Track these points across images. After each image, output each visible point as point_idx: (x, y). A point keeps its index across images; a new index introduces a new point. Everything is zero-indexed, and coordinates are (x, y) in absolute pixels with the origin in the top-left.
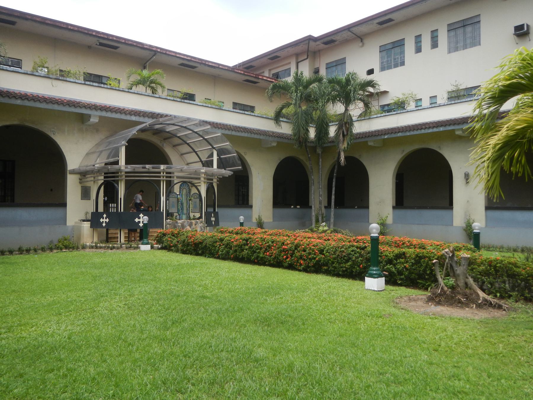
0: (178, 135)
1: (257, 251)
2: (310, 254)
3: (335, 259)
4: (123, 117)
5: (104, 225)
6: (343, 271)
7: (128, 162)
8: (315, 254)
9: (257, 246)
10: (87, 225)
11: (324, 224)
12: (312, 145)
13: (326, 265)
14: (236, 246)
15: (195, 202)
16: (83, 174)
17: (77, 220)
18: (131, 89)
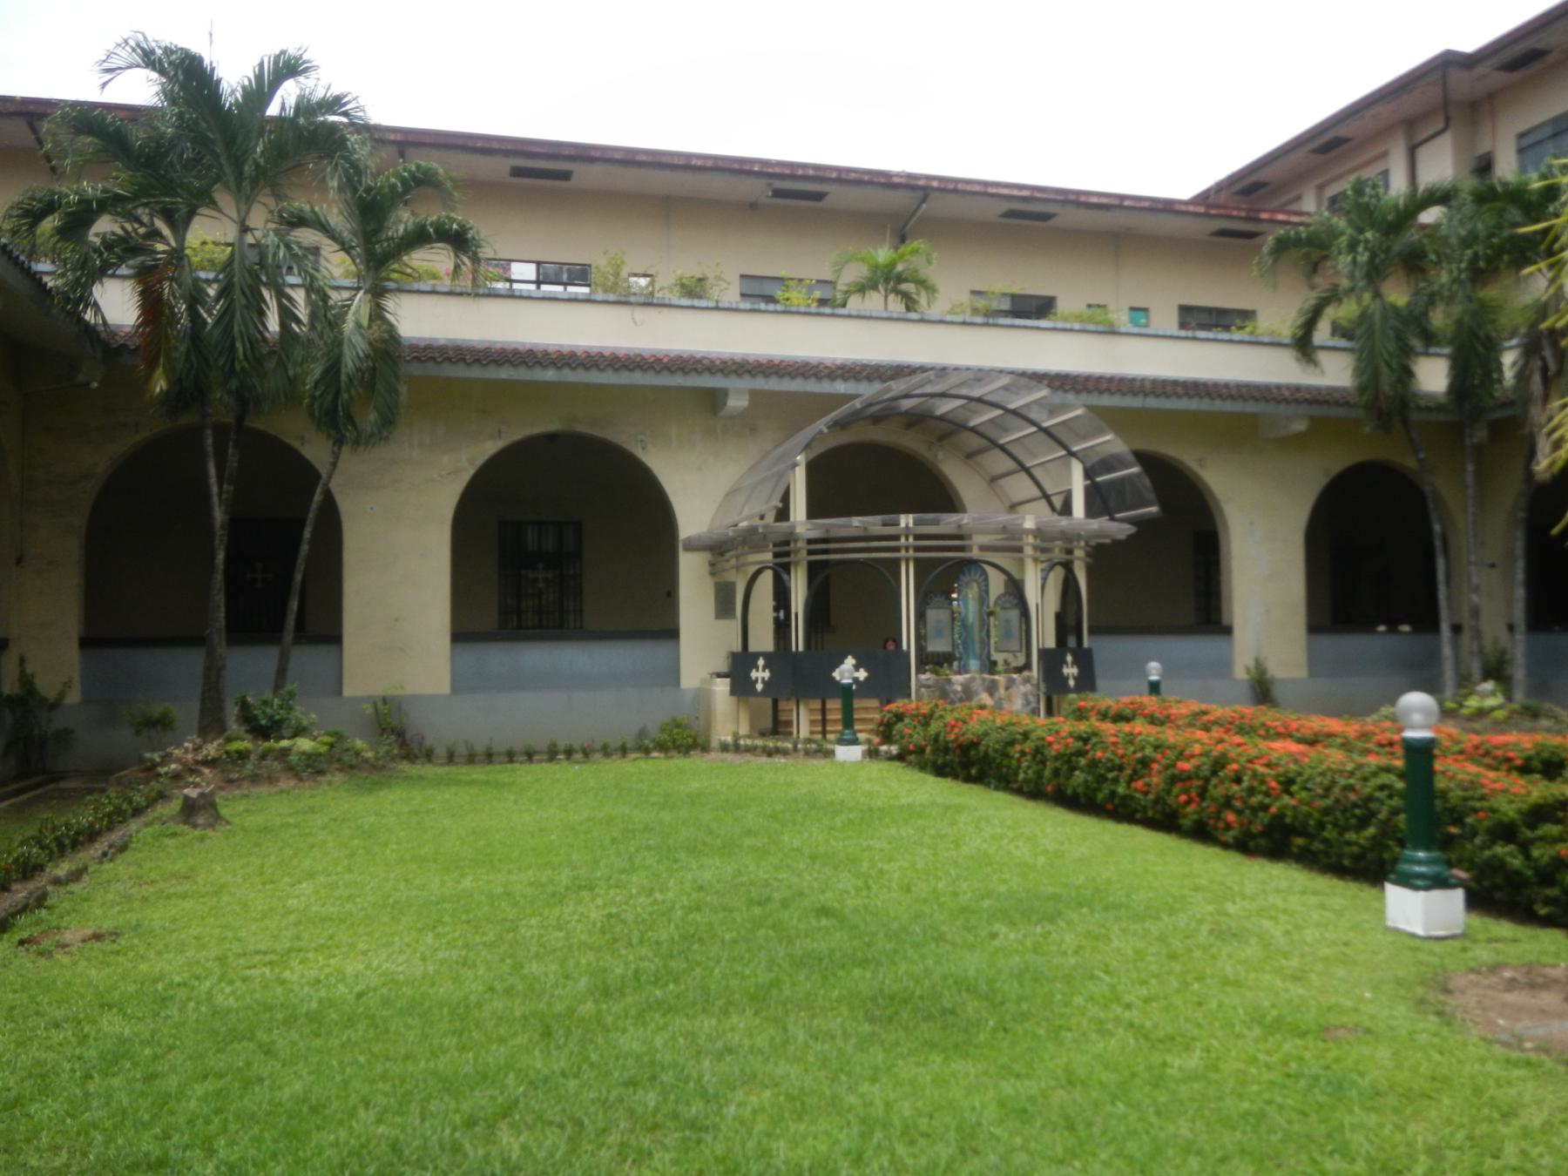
0: (972, 424)
1: (1110, 775)
2: (1251, 791)
3: (1327, 811)
4: (812, 386)
5: (759, 687)
6: (1357, 858)
7: (816, 509)
8: (1267, 794)
9: (1109, 760)
10: (722, 687)
11: (1489, 686)
12: (1442, 417)
13: (1302, 832)
14: (1056, 758)
15: (1008, 621)
16: (717, 549)
17: (705, 675)
18: (844, 305)
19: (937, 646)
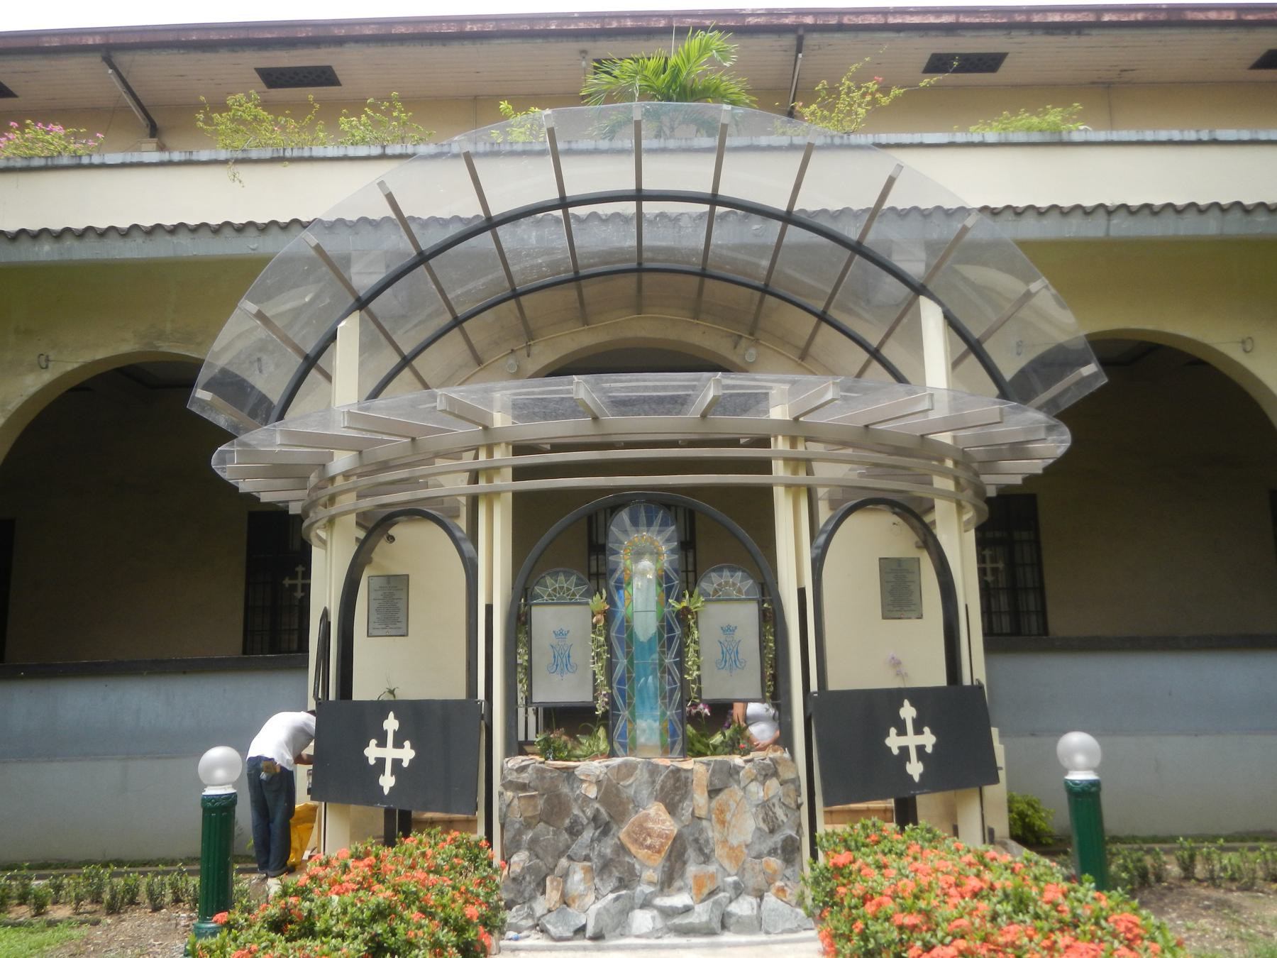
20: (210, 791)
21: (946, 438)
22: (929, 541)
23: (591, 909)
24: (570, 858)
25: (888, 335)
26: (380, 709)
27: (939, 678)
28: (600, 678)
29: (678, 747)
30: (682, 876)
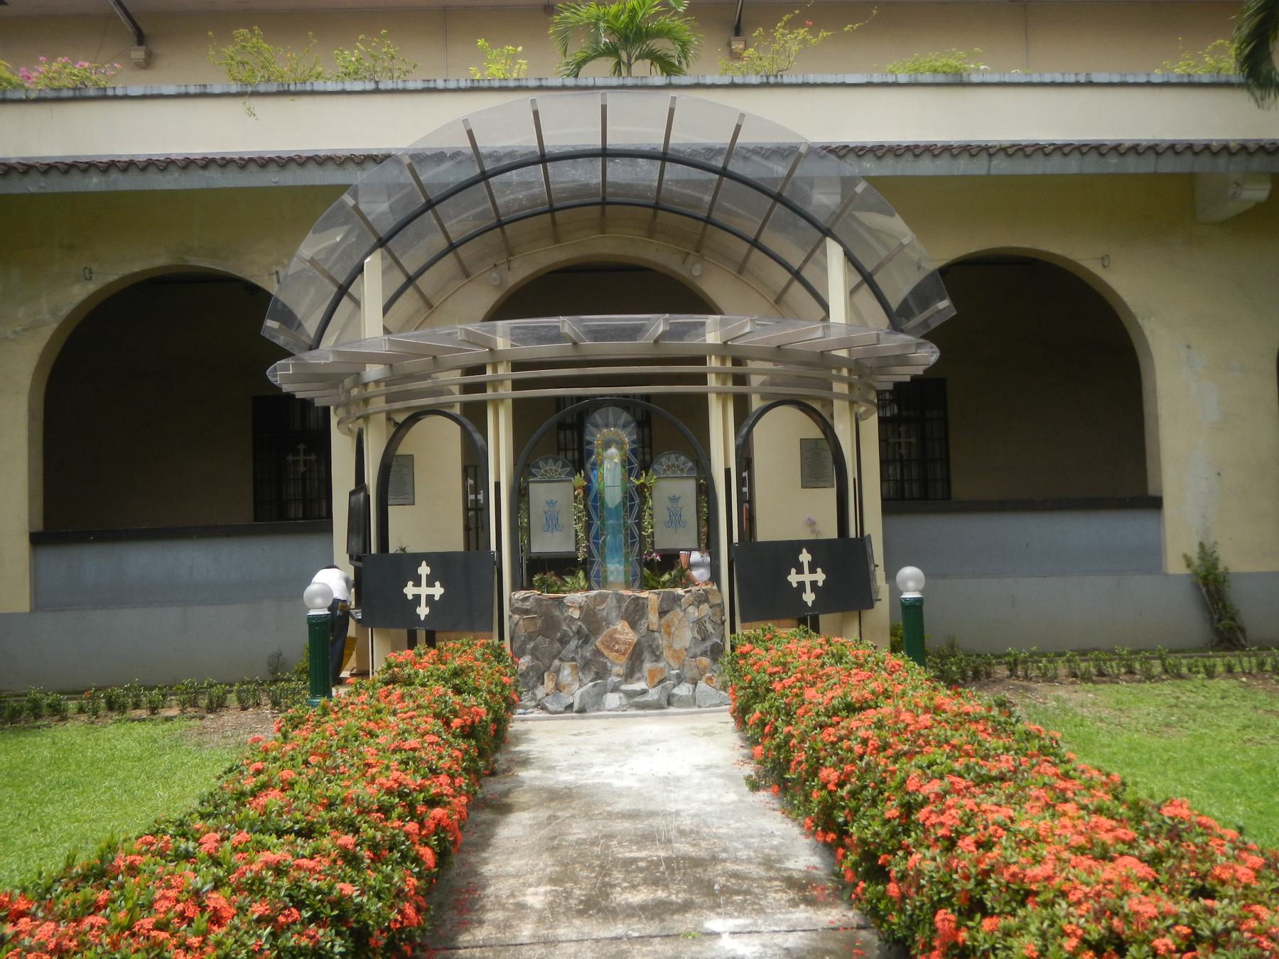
19: (546, 543)
20: (312, 613)
21: (843, 353)
22: (828, 429)
23: (577, 692)
24: (561, 660)
25: (806, 261)
26: (417, 559)
27: (831, 532)
28: (581, 535)
29: (637, 584)
30: (640, 670)
